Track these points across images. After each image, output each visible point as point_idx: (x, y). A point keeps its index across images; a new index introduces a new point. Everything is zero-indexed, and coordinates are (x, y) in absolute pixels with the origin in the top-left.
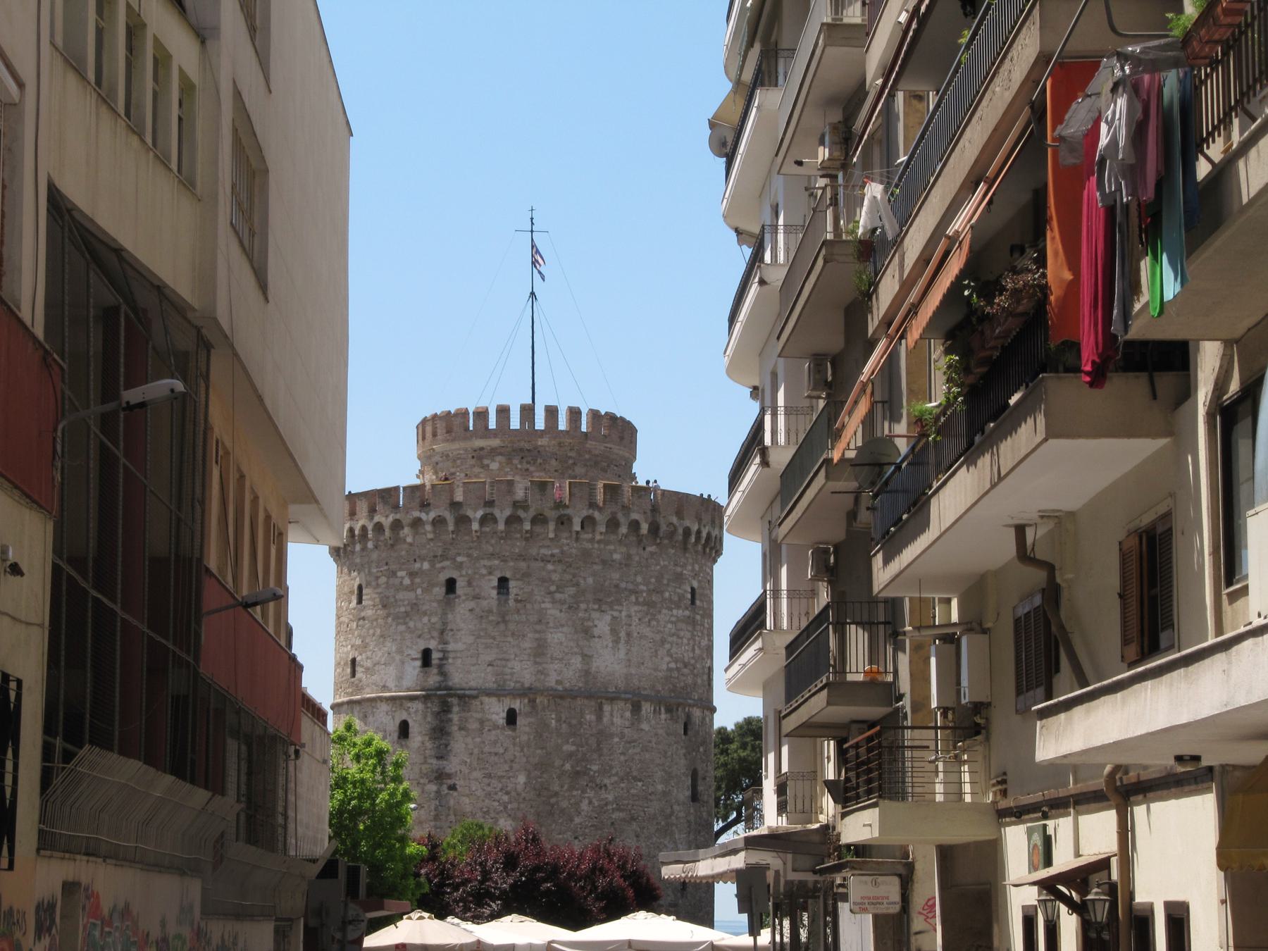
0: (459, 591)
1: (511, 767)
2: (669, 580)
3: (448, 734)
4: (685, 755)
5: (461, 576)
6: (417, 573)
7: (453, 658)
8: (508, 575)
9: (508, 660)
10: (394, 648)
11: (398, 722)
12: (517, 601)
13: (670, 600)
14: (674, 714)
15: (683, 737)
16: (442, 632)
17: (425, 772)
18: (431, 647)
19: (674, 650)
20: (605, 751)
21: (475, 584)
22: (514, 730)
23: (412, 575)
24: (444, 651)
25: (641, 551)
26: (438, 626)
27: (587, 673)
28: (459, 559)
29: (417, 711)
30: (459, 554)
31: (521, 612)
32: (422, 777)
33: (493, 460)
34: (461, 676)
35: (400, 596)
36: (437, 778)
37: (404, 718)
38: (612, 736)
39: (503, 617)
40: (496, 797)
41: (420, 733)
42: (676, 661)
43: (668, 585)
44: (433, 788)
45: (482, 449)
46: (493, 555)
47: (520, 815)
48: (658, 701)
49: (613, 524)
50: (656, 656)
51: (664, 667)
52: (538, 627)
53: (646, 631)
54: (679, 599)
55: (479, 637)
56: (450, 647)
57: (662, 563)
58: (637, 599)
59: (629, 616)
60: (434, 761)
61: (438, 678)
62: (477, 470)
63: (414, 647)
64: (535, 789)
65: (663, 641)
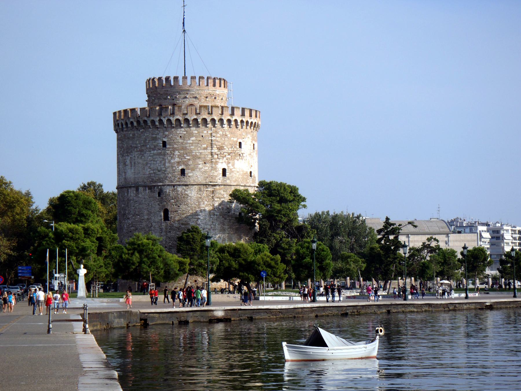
2: (149, 141)
4: (158, 204)
13: (150, 148)
14: (153, 190)
15: (158, 198)
19: (152, 166)
20: (129, 206)
25: (138, 132)
27: (125, 179)
38: (131, 200)
42: (153, 170)
43: (148, 143)
48: (145, 186)
49: (126, 124)
50: (144, 169)
51: (148, 173)
53: (140, 161)
54: (155, 147)
57: (146, 135)
58: (137, 149)
59: (135, 156)
65: (147, 164)
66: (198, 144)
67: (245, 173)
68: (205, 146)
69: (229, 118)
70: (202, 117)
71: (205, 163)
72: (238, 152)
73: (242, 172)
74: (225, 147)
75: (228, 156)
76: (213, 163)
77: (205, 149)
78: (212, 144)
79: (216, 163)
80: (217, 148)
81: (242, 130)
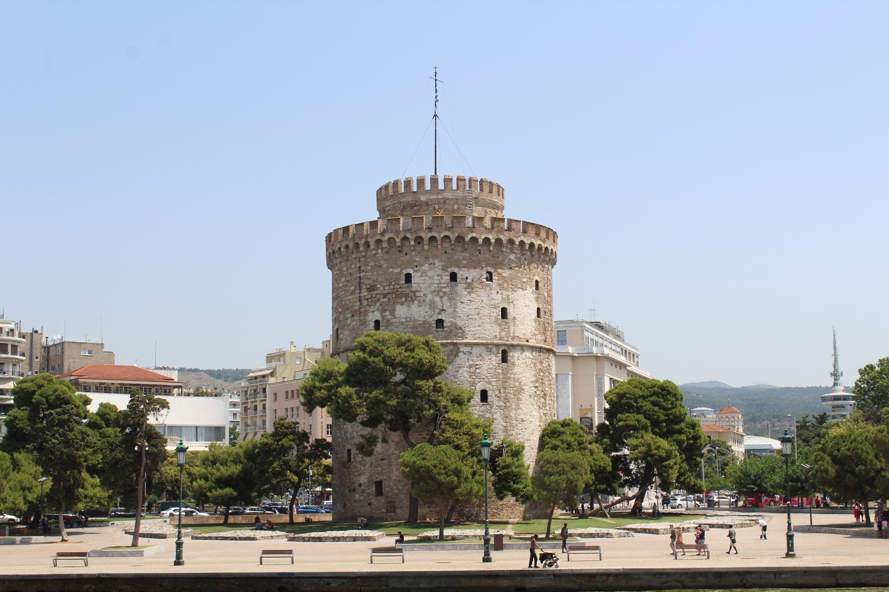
66: (347, 286)
67: (420, 324)
68: (353, 288)
69: (379, 237)
70: (344, 245)
71: (353, 316)
72: (404, 290)
73: (413, 323)
74: (378, 286)
75: (382, 300)
76: (362, 314)
77: (353, 293)
78: (360, 283)
79: (366, 313)
80: (366, 288)
81: (413, 253)
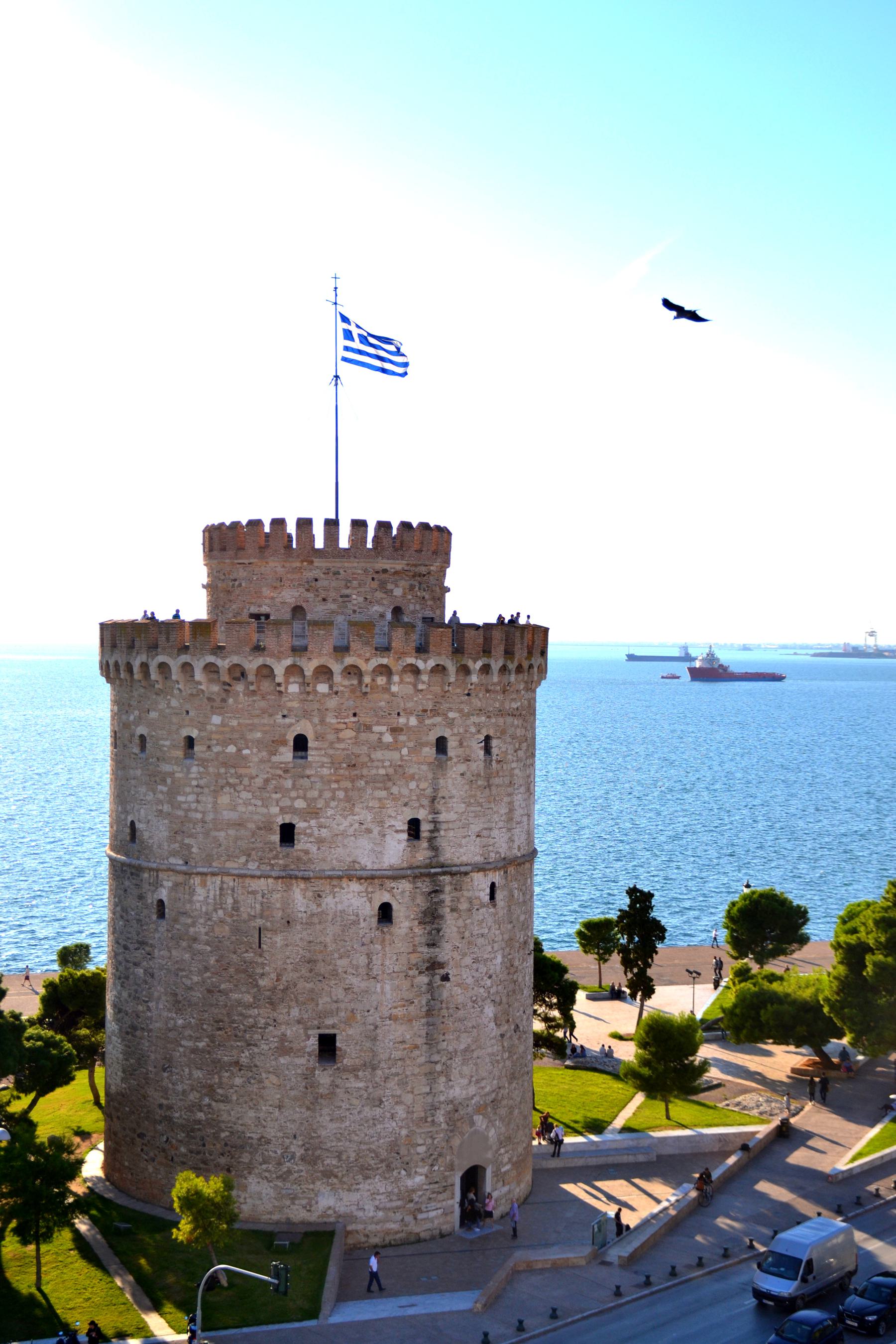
0: (451, 753)
1: (493, 948)
3: (441, 917)
5: (454, 735)
6: (402, 730)
7: (445, 830)
8: (491, 734)
9: (491, 829)
10: (369, 818)
11: (377, 905)
12: (499, 762)
16: (433, 800)
17: (414, 962)
18: (420, 817)
21: (465, 744)
22: (494, 906)
23: (395, 731)
24: (435, 822)
26: (429, 791)
28: (451, 715)
29: (403, 892)
30: (450, 709)
31: (501, 774)
32: (410, 969)
33: (397, 586)
34: (453, 850)
35: (378, 755)
36: (427, 969)
37: (385, 900)
39: (488, 781)
40: (482, 983)
41: (407, 917)
44: (424, 979)
45: (385, 571)
46: (481, 710)
47: (498, 999)
52: (510, 790)
55: (469, 805)
56: (442, 817)
60: (425, 949)
61: (429, 854)
62: (379, 595)
63: (399, 817)
64: (507, 968)
